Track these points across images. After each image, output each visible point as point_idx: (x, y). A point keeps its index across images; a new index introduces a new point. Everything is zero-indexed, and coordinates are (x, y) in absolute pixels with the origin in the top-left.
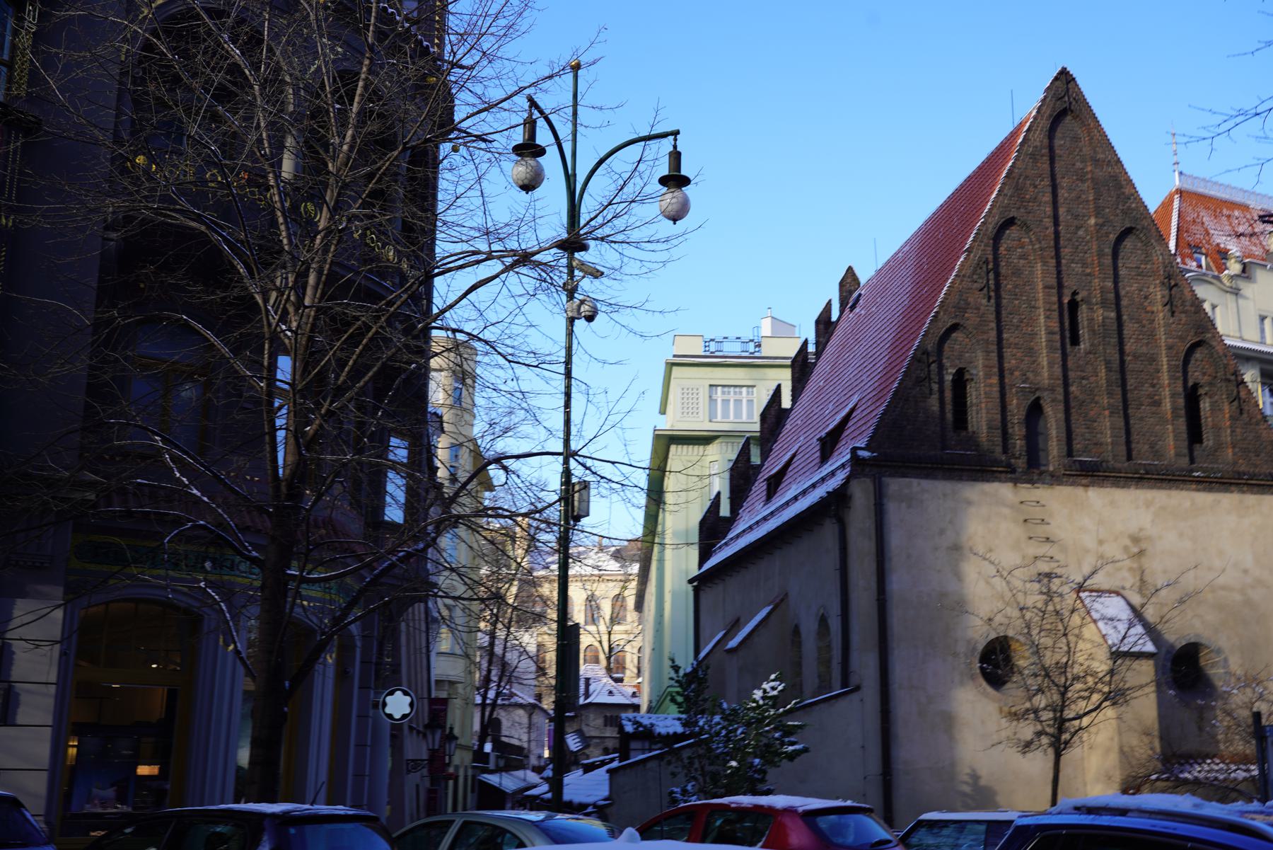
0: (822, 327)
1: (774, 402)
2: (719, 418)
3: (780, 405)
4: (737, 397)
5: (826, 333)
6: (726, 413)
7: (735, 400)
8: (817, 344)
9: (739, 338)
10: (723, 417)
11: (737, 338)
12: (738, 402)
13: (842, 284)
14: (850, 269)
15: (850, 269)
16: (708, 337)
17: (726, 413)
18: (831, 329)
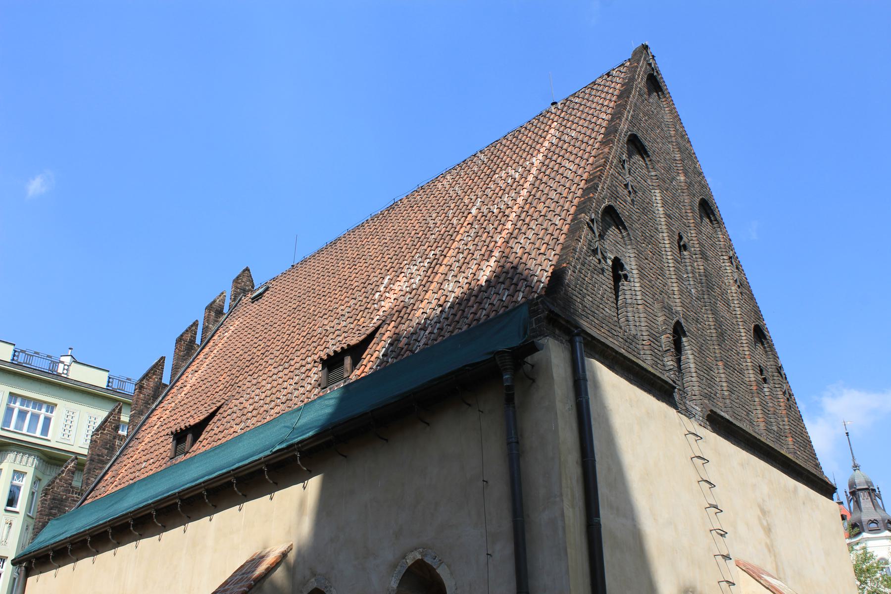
0: (213, 314)
1: (154, 374)
2: (12, 428)
3: (161, 379)
4: (36, 411)
5: (217, 321)
6: (19, 426)
7: (33, 415)
8: (205, 329)
9: (51, 357)
10: (16, 428)
11: (48, 356)
12: (35, 417)
13: (236, 280)
14: (247, 269)
15: (247, 269)
16: (20, 347)
17: (19, 426)
18: (222, 319)
